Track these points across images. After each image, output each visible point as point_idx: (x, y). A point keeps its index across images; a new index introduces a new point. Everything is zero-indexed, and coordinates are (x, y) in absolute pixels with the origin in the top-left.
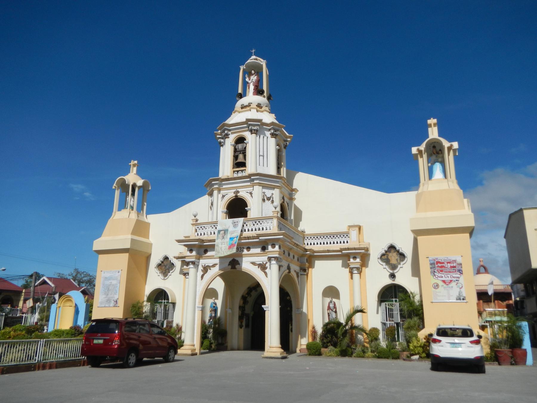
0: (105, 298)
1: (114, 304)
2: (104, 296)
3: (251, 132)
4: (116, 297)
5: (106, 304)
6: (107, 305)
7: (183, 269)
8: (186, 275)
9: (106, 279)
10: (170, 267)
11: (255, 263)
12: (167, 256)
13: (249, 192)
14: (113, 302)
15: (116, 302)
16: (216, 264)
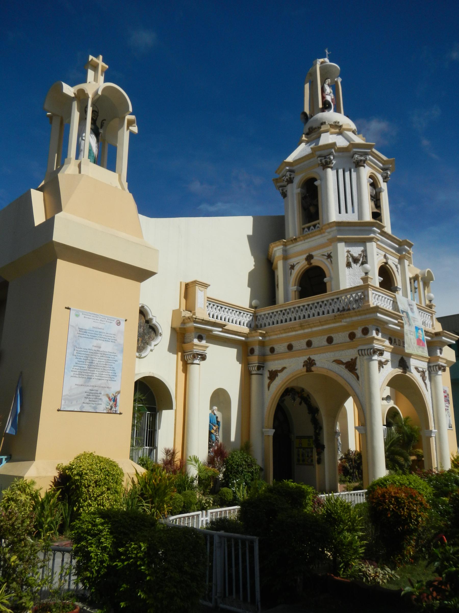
0: (81, 385)
1: (110, 408)
2: (80, 381)
3: (383, 179)
4: (114, 388)
5: (83, 403)
6: (87, 408)
7: (196, 345)
8: (198, 357)
9: (82, 332)
10: (146, 331)
11: (418, 369)
12: (145, 306)
13: (395, 263)
14: (108, 399)
15: (115, 400)
16: (387, 361)
